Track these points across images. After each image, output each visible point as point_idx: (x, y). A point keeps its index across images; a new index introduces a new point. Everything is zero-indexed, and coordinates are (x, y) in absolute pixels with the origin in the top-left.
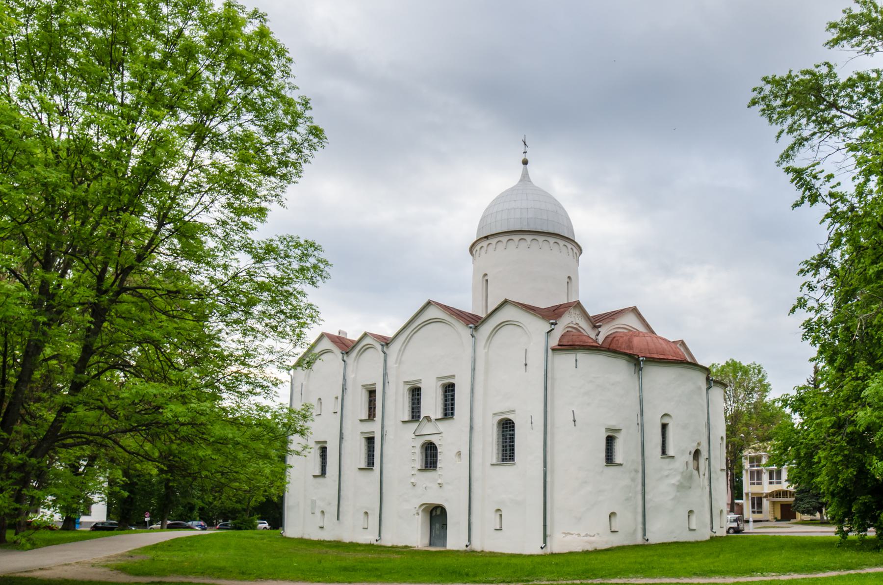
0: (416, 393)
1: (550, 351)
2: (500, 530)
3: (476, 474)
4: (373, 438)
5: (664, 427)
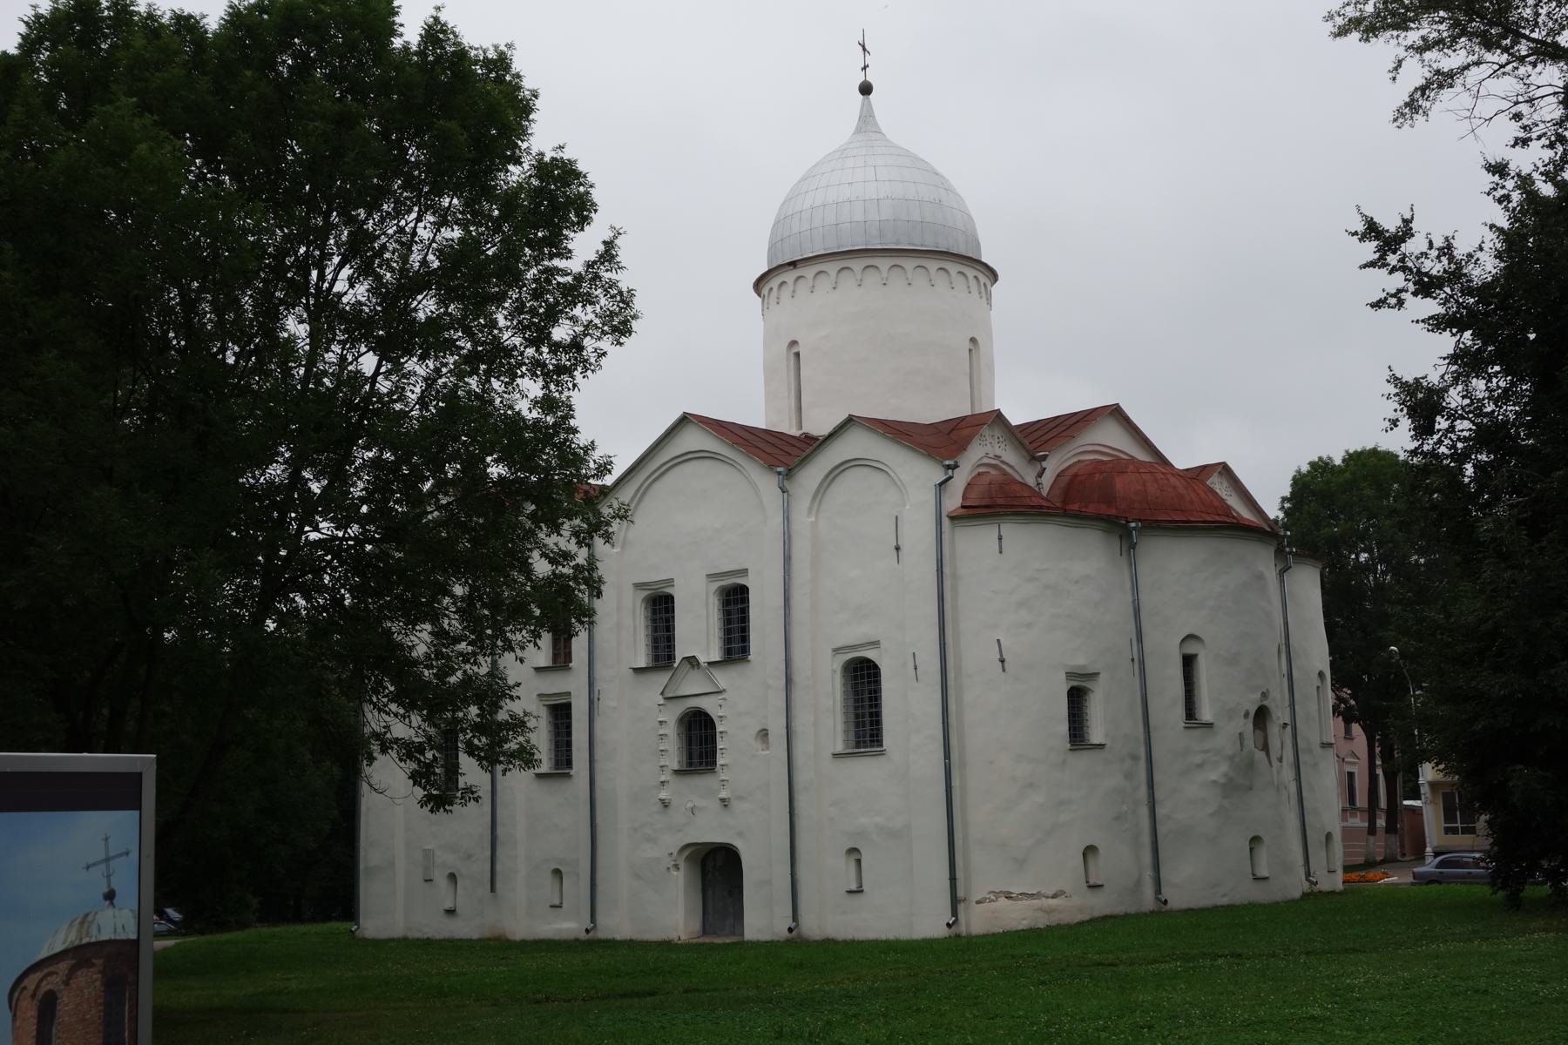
0: (661, 607)
1: (946, 521)
2: (859, 891)
3: (801, 778)
4: (568, 706)
5: (1189, 662)
